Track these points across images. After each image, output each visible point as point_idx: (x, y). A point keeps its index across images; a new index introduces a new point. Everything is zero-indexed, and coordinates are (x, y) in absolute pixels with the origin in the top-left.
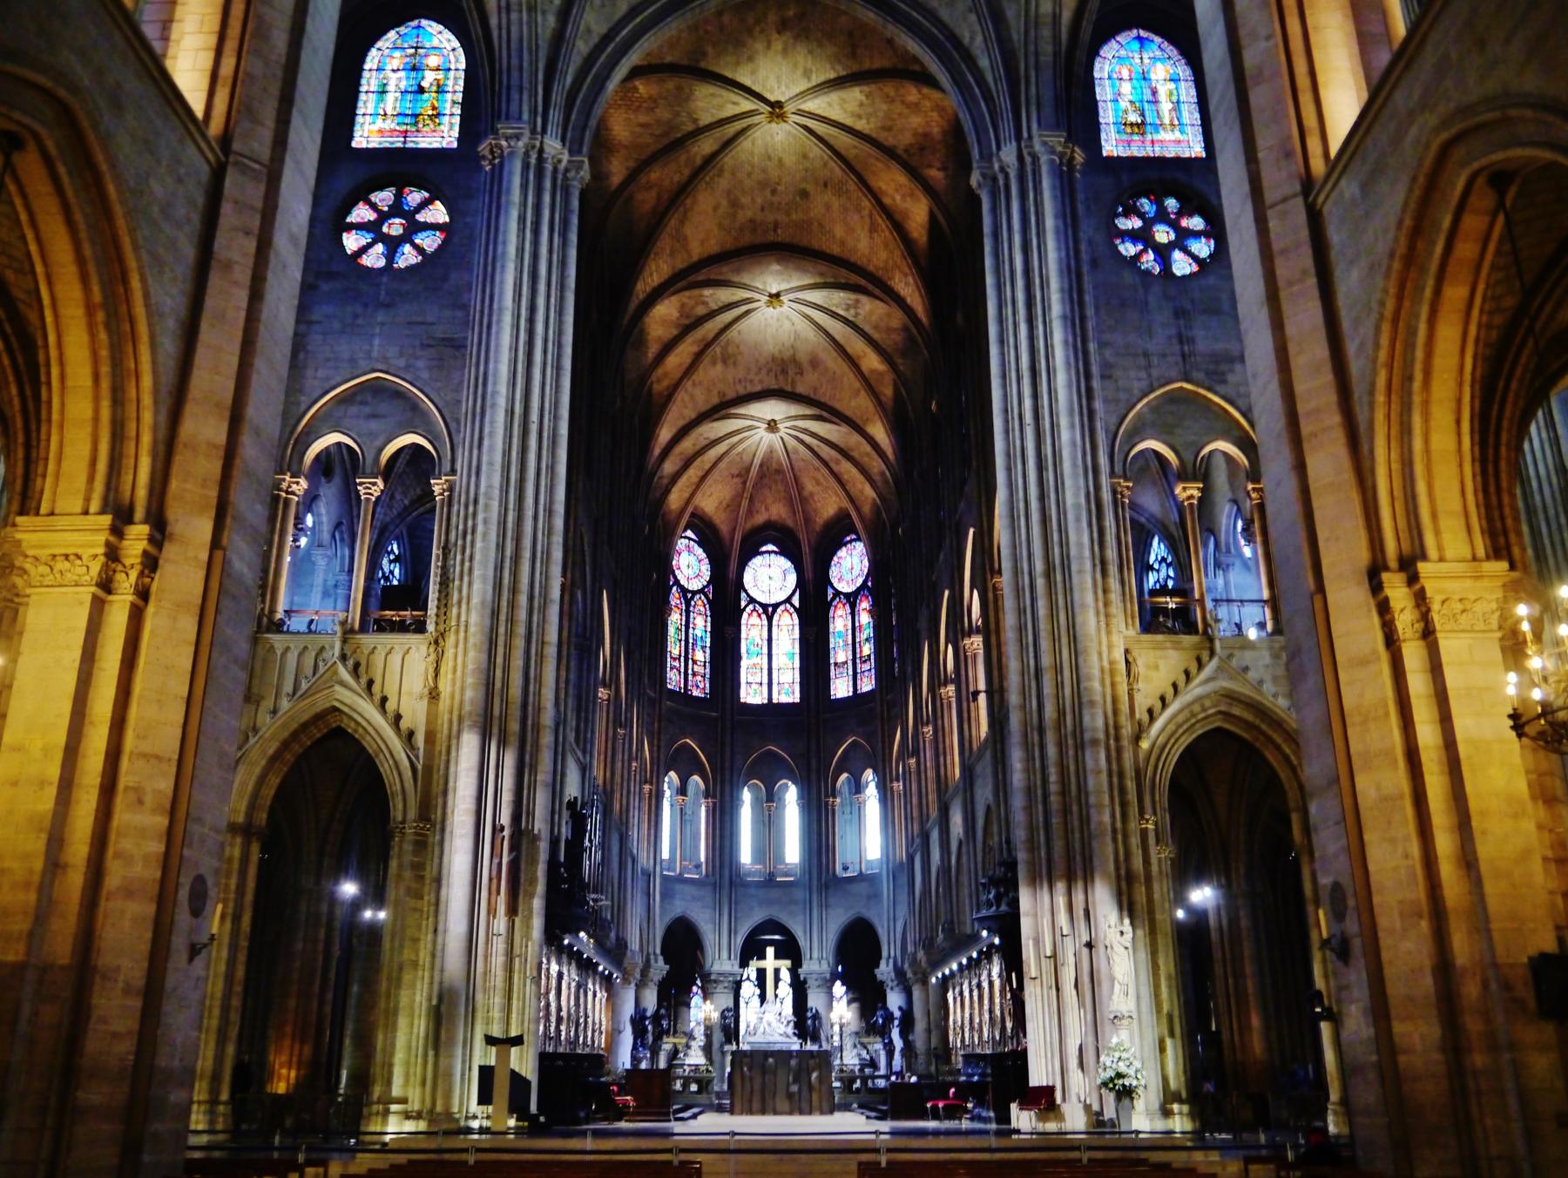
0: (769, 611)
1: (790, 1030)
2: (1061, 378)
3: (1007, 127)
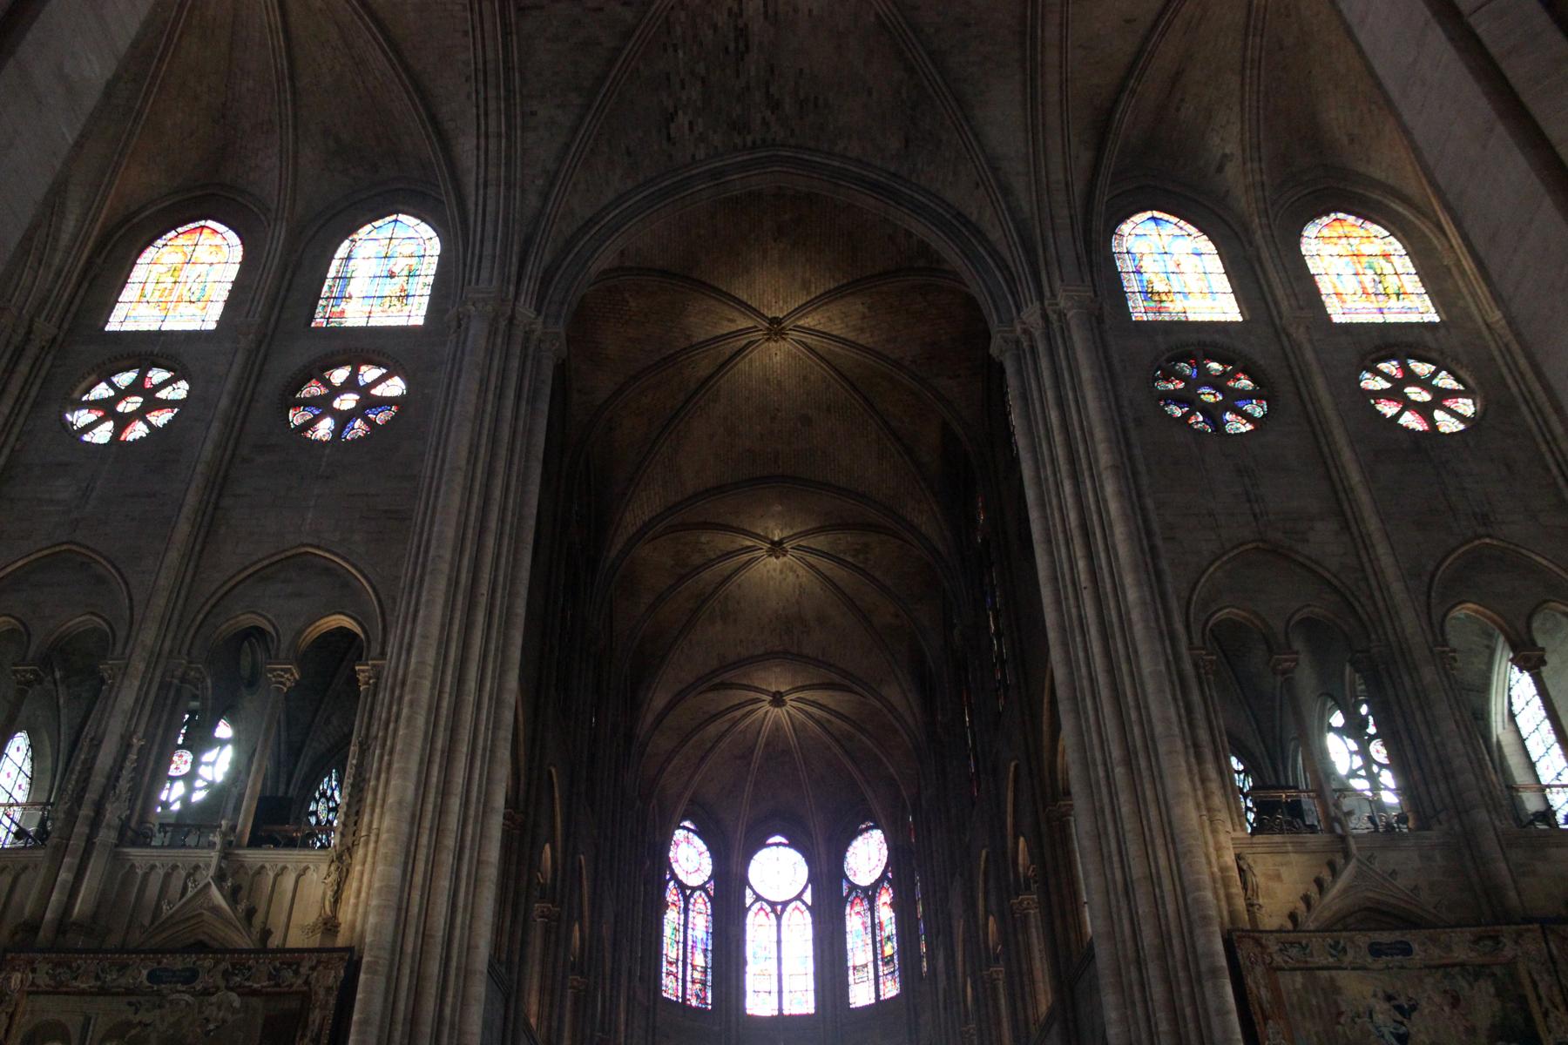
0: (778, 909)
2: (1119, 532)
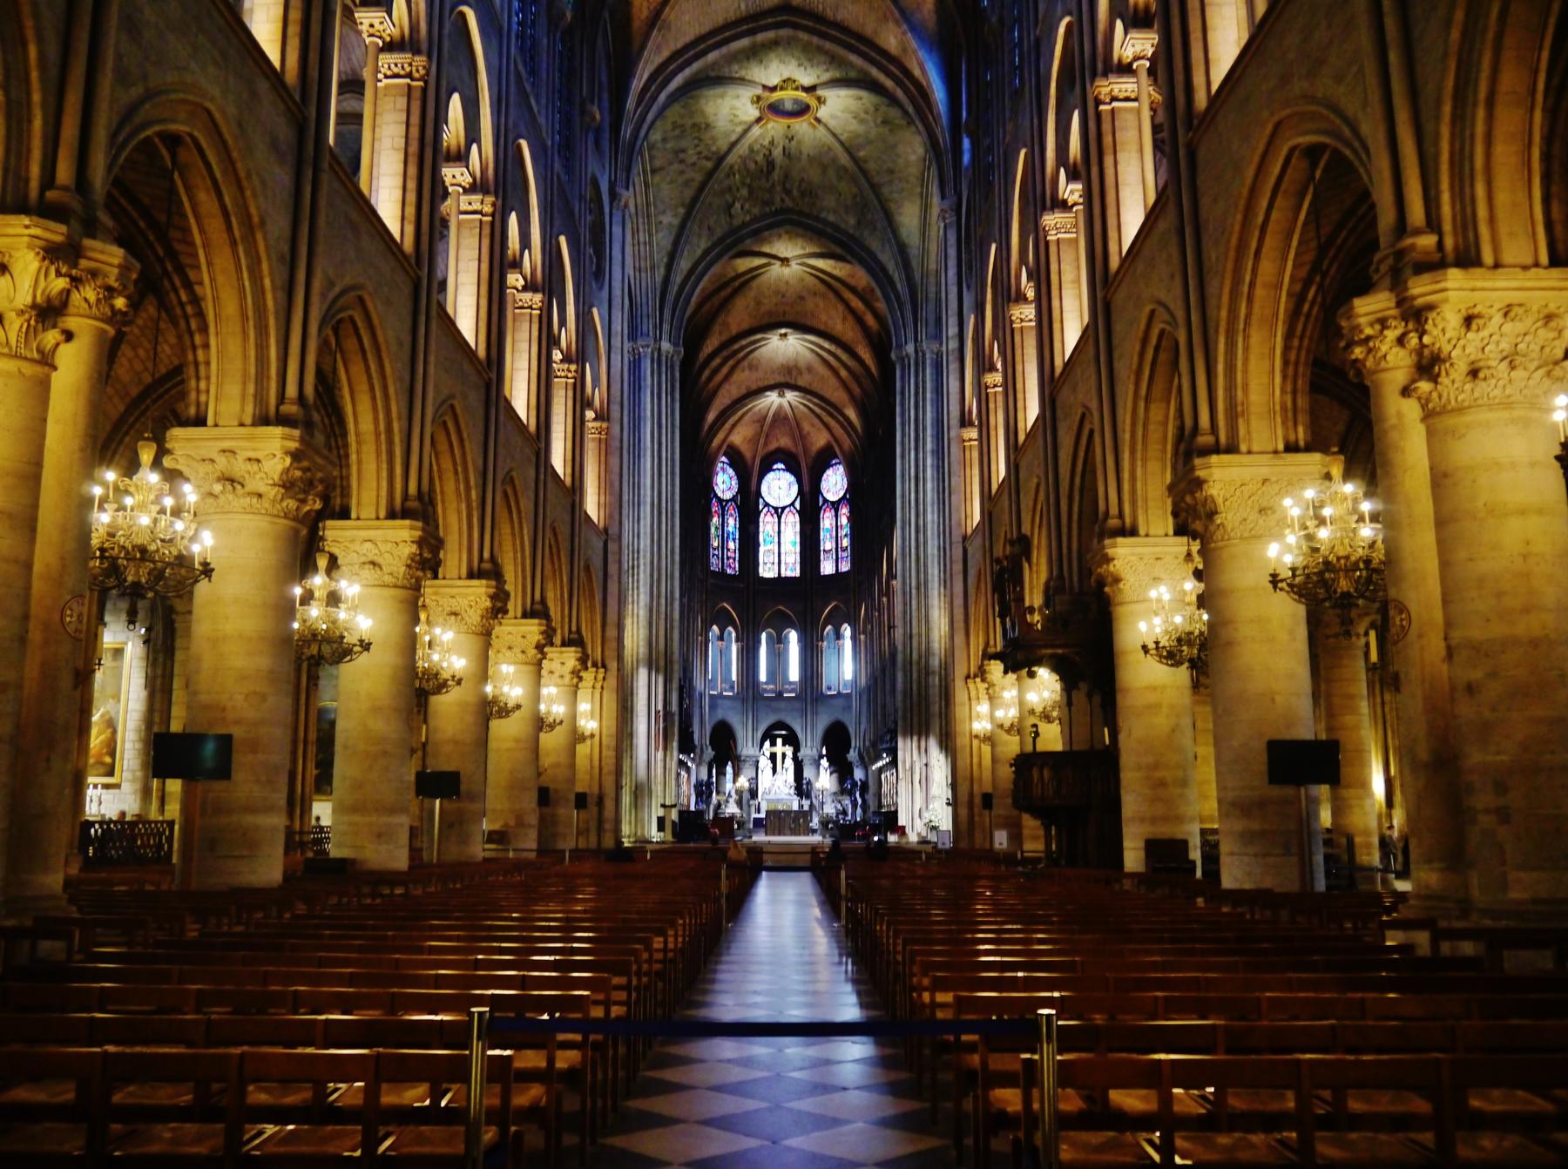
0: (779, 512)
1: (792, 791)
3: (910, 335)
